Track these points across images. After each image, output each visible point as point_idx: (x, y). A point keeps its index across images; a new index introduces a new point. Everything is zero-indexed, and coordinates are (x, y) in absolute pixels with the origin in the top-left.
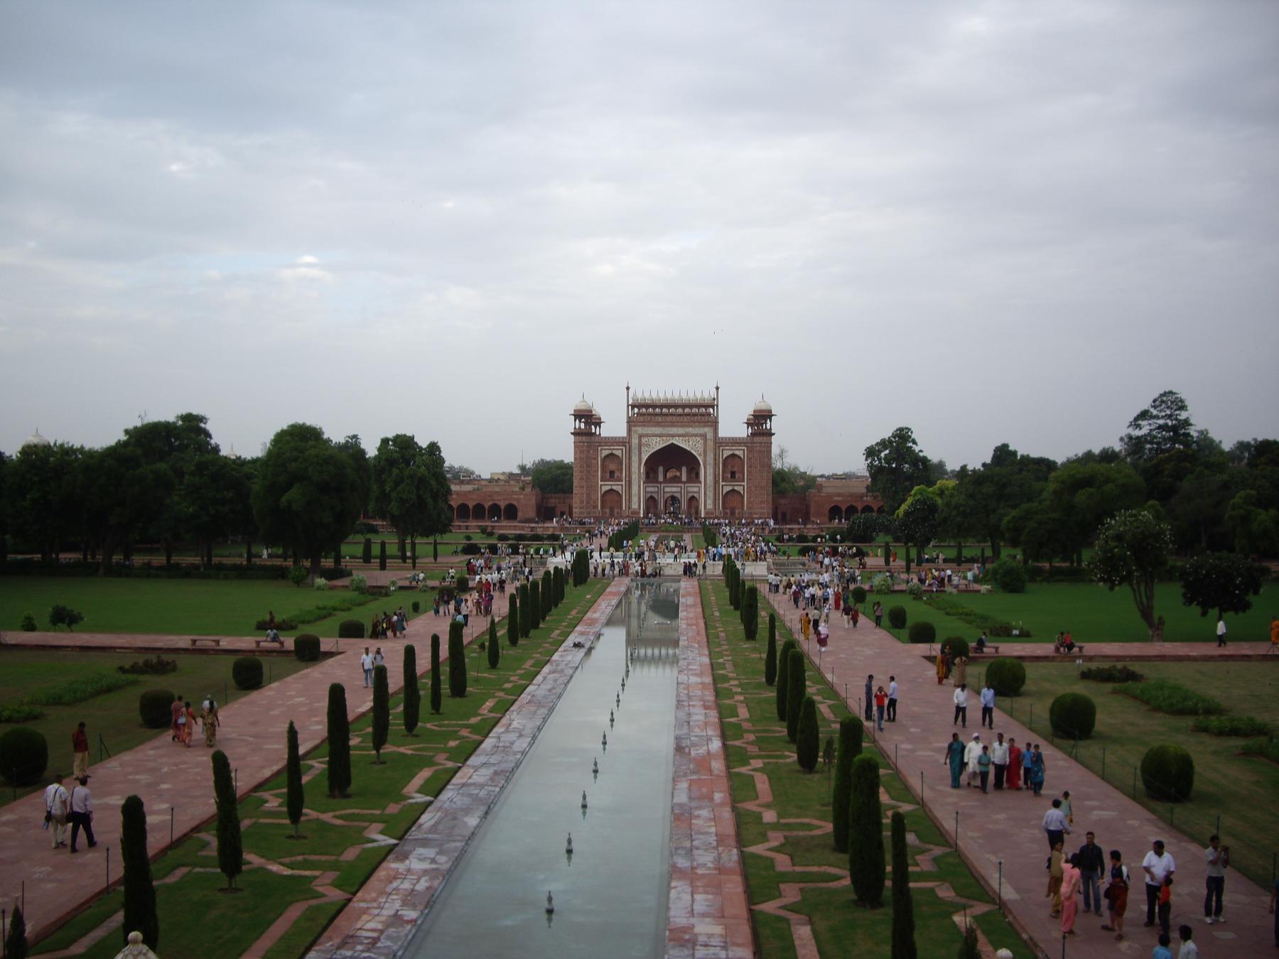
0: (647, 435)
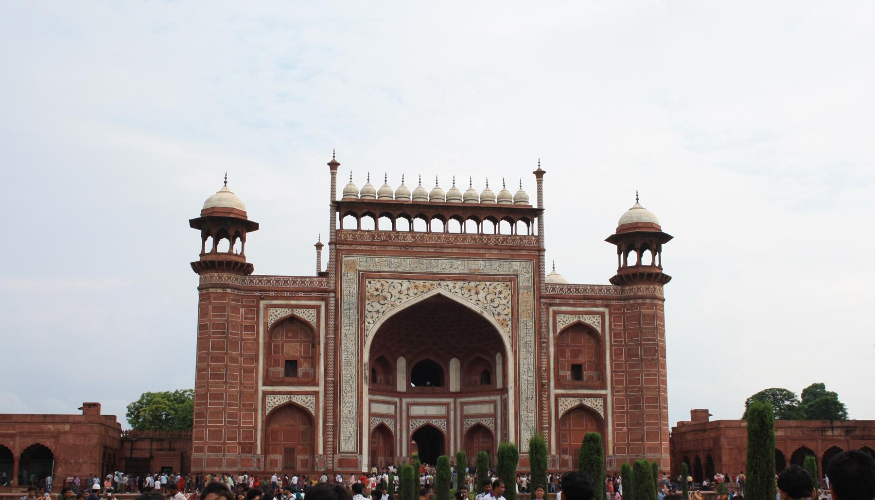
0: (379, 275)
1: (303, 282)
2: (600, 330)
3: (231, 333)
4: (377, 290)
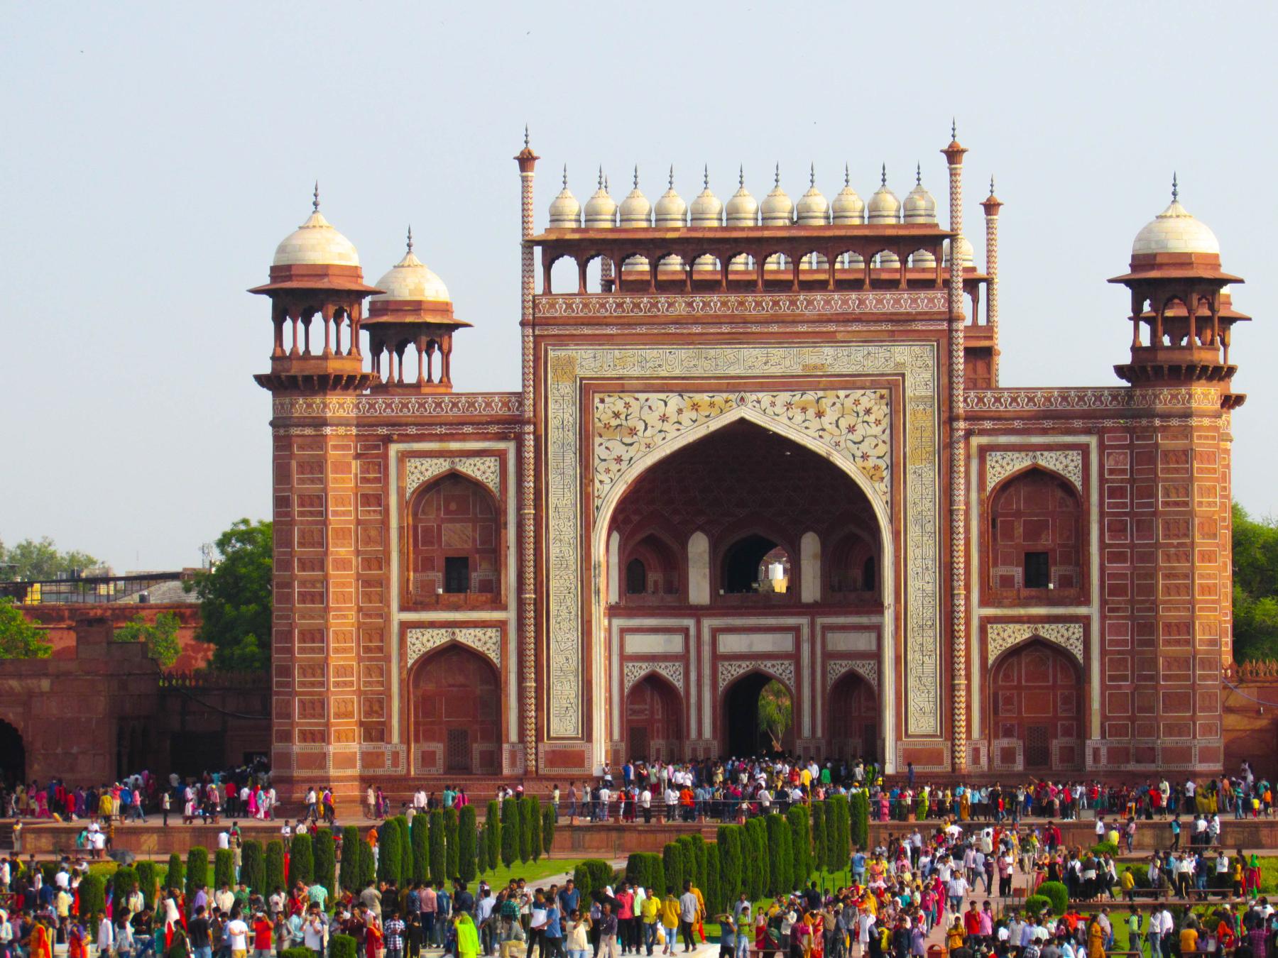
0: (619, 386)
1: (472, 405)
2: (1078, 485)
3: (336, 513)
4: (617, 415)
